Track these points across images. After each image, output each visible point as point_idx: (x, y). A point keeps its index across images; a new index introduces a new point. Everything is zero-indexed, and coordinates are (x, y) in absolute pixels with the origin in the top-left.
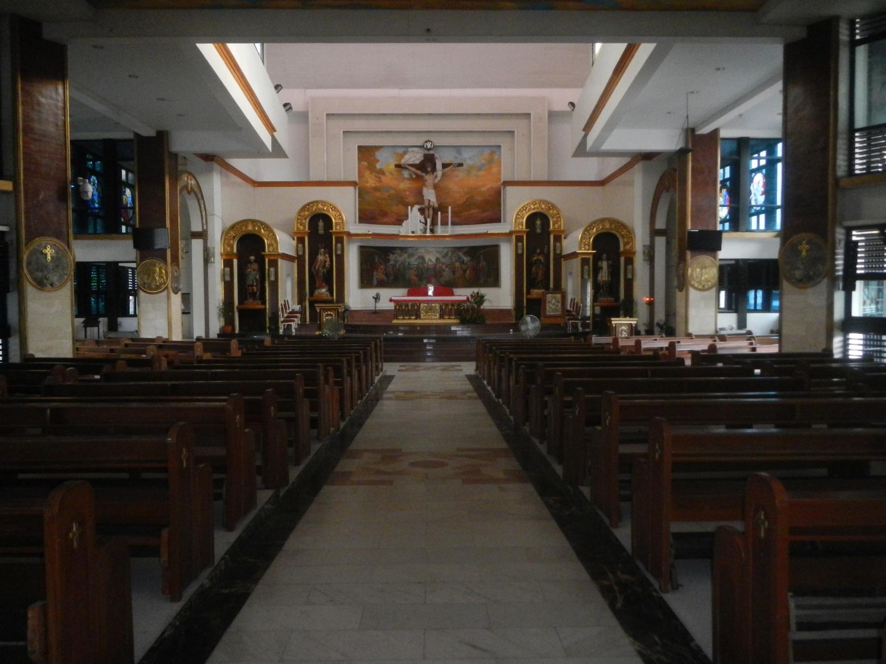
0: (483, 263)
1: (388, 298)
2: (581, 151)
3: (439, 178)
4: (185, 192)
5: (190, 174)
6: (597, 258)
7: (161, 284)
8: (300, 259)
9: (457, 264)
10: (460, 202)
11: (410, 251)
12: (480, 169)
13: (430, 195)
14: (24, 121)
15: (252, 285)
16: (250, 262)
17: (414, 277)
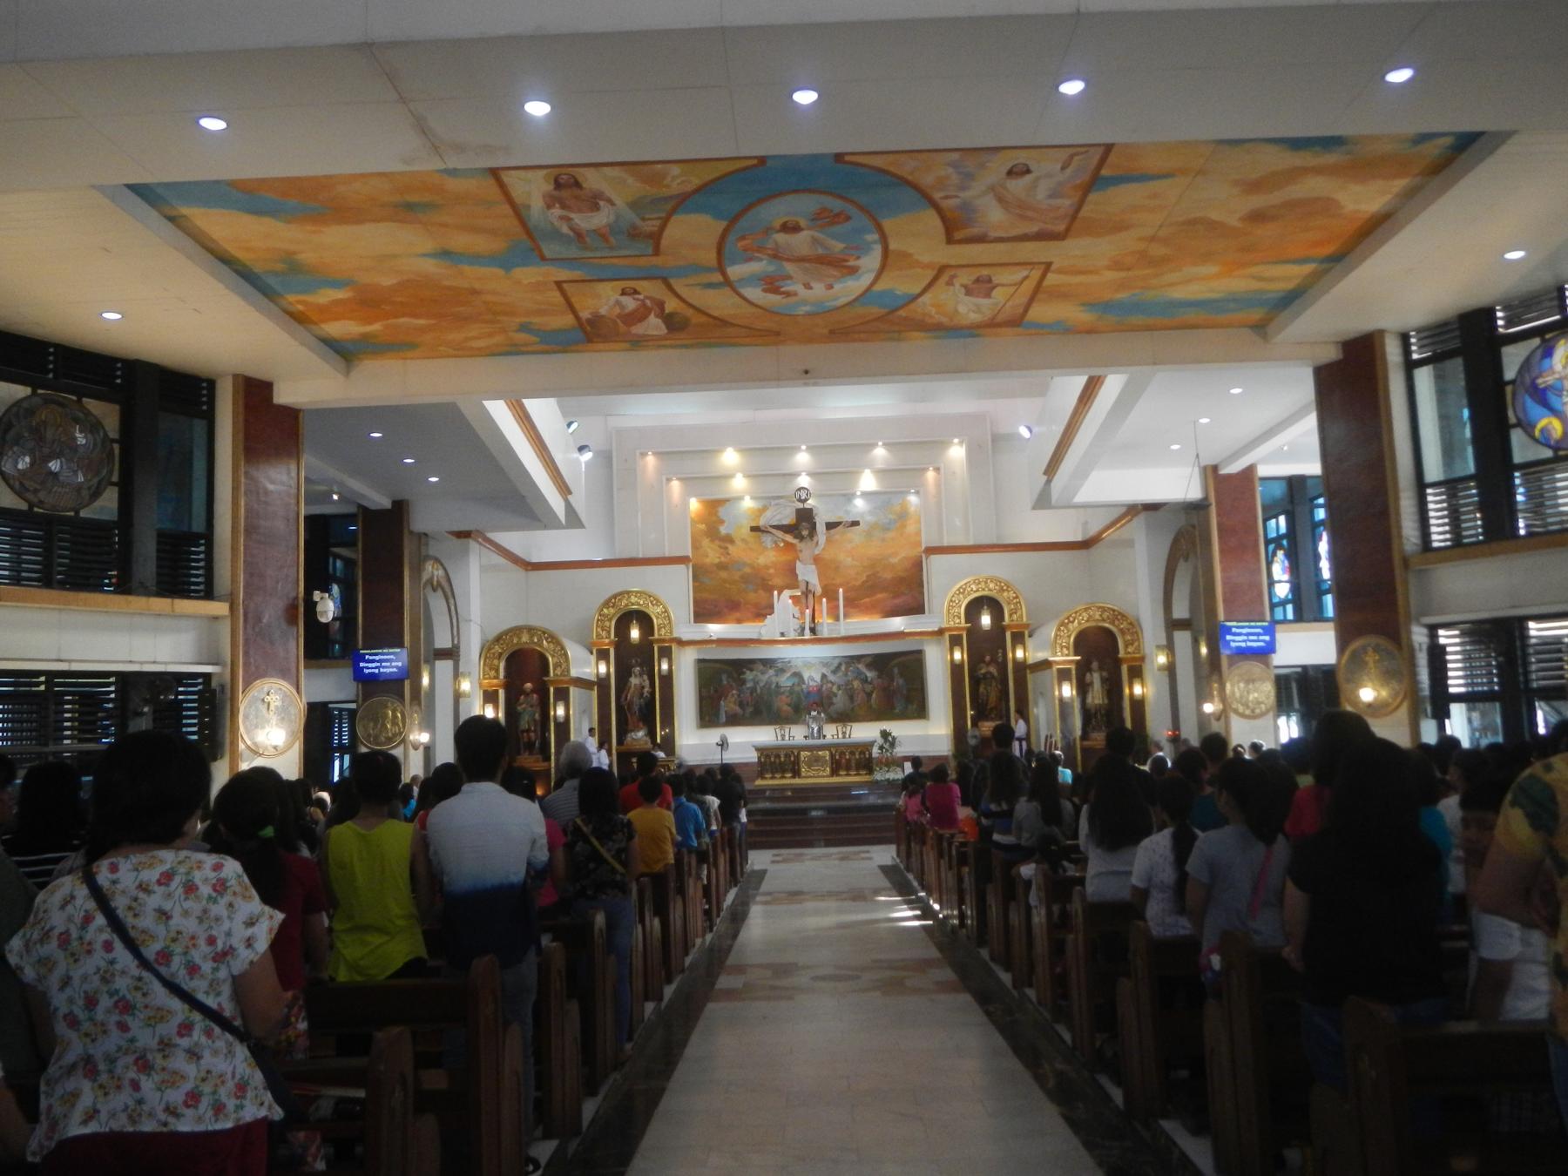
0: (899, 681)
1: (745, 742)
2: (1043, 501)
4: (429, 589)
5: (437, 560)
6: (1083, 668)
7: (395, 735)
8: (602, 684)
9: (856, 684)
10: (858, 583)
14: (246, 518)
15: (528, 731)
16: (523, 692)
17: (786, 708)
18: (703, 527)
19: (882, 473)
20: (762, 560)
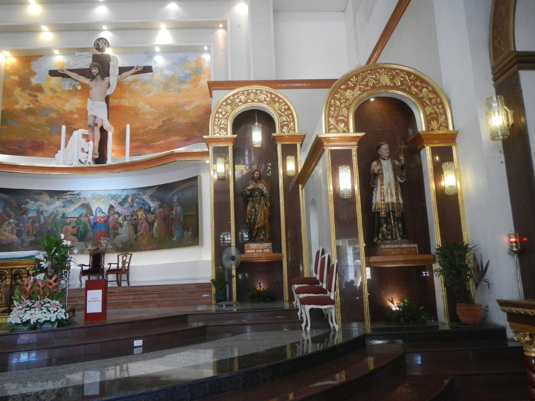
3: (113, 86)
9: (141, 214)
11: (68, 197)
12: (182, 82)
13: (98, 110)
18: (16, 78)
20: (68, 107)
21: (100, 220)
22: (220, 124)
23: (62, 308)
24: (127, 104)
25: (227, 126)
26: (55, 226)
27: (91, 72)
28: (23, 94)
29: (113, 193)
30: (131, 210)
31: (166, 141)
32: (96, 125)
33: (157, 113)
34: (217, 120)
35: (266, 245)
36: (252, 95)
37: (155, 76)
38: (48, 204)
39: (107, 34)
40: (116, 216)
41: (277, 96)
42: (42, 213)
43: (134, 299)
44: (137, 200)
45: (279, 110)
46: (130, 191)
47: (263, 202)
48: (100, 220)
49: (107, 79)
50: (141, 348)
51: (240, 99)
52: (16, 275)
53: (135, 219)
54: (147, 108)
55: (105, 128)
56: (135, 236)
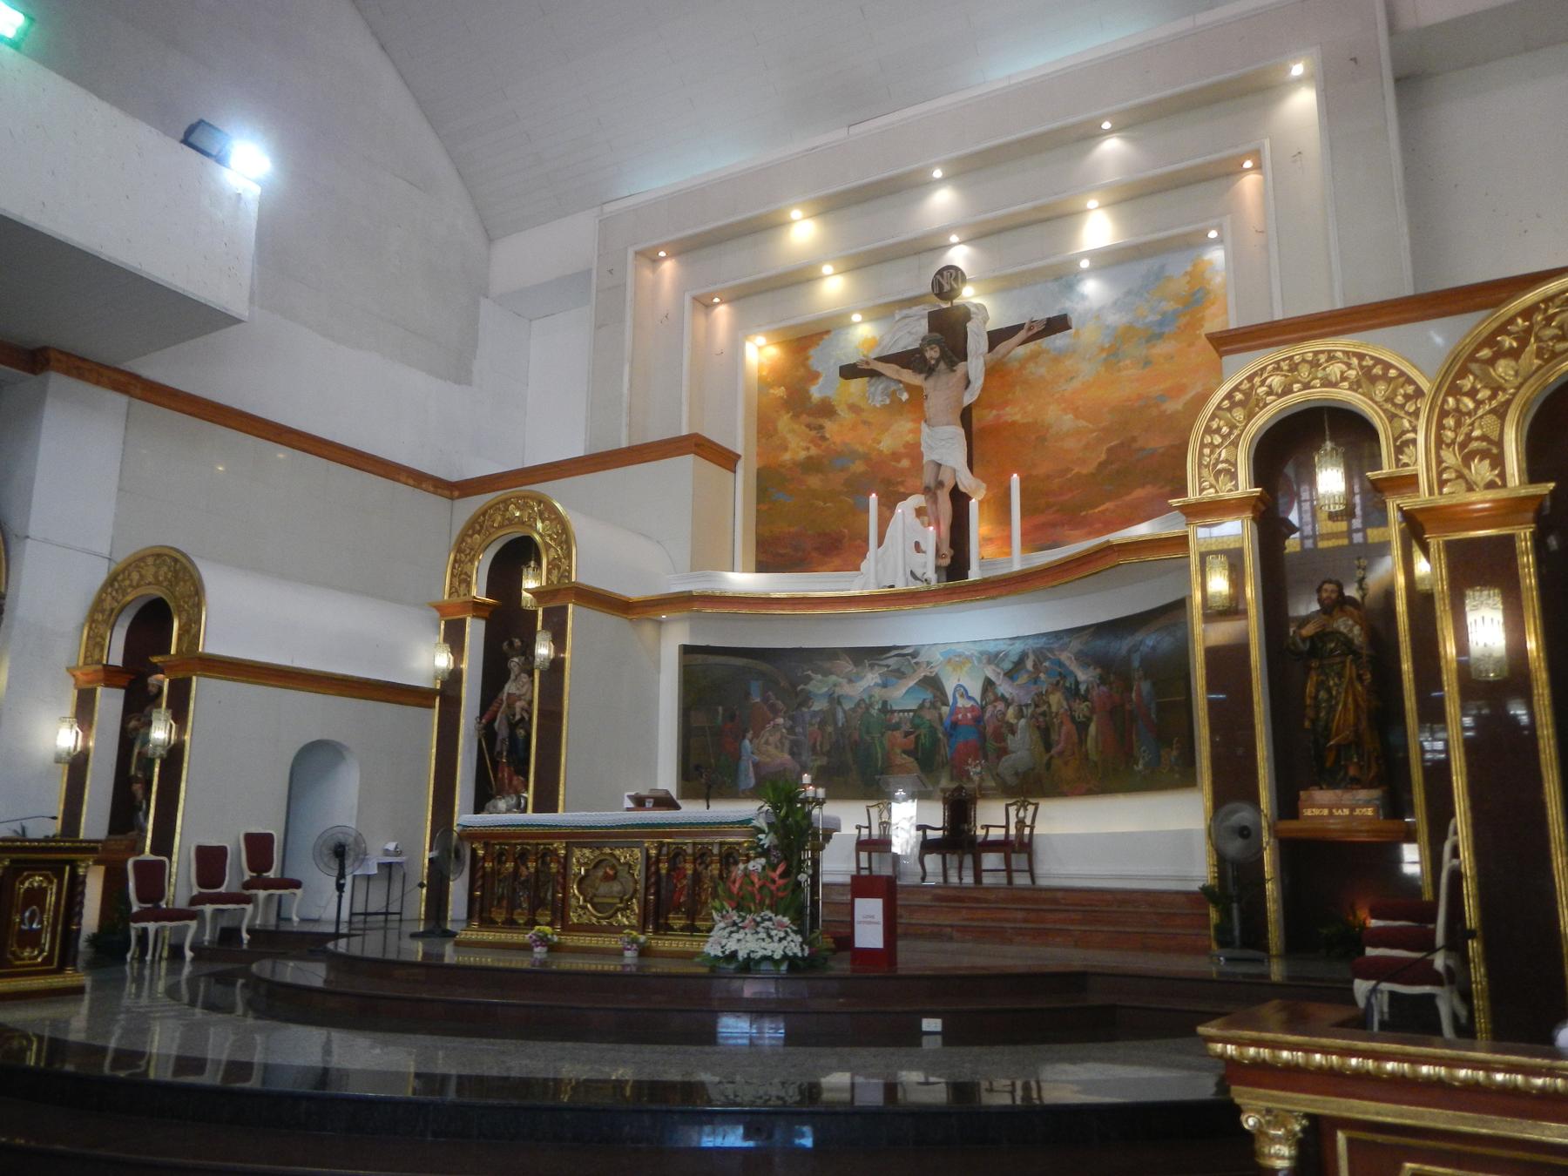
3: (978, 382)
8: (448, 691)
9: (1056, 700)
10: (1090, 468)
11: (893, 662)
12: (1153, 337)
13: (946, 448)
18: (780, 392)
19: (1132, 196)
20: (887, 444)
21: (965, 716)
22: (1218, 462)
23: (796, 932)
24: (1018, 417)
25: (1235, 465)
26: (868, 732)
27: (925, 360)
28: (796, 427)
29: (992, 648)
30: (1034, 689)
31: (1119, 502)
32: (940, 484)
33: (1092, 431)
34: (1207, 451)
35: (1363, 794)
36: (1304, 372)
37: (1085, 335)
38: (850, 681)
39: (959, 255)
40: (1000, 706)
41: (1378, 361)
42: (839, 703)
43: (1025, 921)
44: (1047, 664)
45: (1386, 400)
46: (1030, 642)
47: (1350, 670)
48: (965, 716)
49: (961, 367)
50: (939, 1038)
51: (1270, 387)
52: (729, 857)
53: (1044, 714)
54: (1068, 421)
55: (961, 488)
56: (1046, 758)
